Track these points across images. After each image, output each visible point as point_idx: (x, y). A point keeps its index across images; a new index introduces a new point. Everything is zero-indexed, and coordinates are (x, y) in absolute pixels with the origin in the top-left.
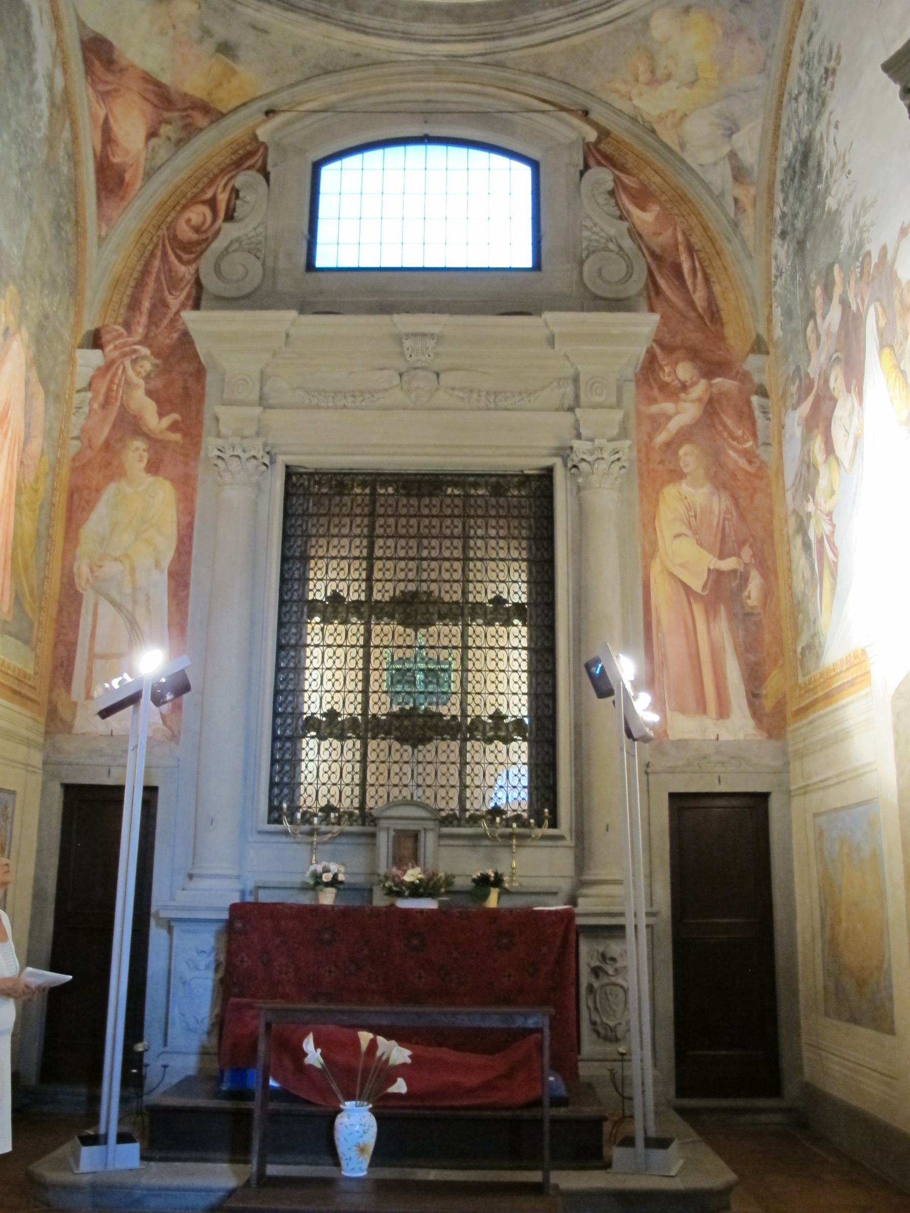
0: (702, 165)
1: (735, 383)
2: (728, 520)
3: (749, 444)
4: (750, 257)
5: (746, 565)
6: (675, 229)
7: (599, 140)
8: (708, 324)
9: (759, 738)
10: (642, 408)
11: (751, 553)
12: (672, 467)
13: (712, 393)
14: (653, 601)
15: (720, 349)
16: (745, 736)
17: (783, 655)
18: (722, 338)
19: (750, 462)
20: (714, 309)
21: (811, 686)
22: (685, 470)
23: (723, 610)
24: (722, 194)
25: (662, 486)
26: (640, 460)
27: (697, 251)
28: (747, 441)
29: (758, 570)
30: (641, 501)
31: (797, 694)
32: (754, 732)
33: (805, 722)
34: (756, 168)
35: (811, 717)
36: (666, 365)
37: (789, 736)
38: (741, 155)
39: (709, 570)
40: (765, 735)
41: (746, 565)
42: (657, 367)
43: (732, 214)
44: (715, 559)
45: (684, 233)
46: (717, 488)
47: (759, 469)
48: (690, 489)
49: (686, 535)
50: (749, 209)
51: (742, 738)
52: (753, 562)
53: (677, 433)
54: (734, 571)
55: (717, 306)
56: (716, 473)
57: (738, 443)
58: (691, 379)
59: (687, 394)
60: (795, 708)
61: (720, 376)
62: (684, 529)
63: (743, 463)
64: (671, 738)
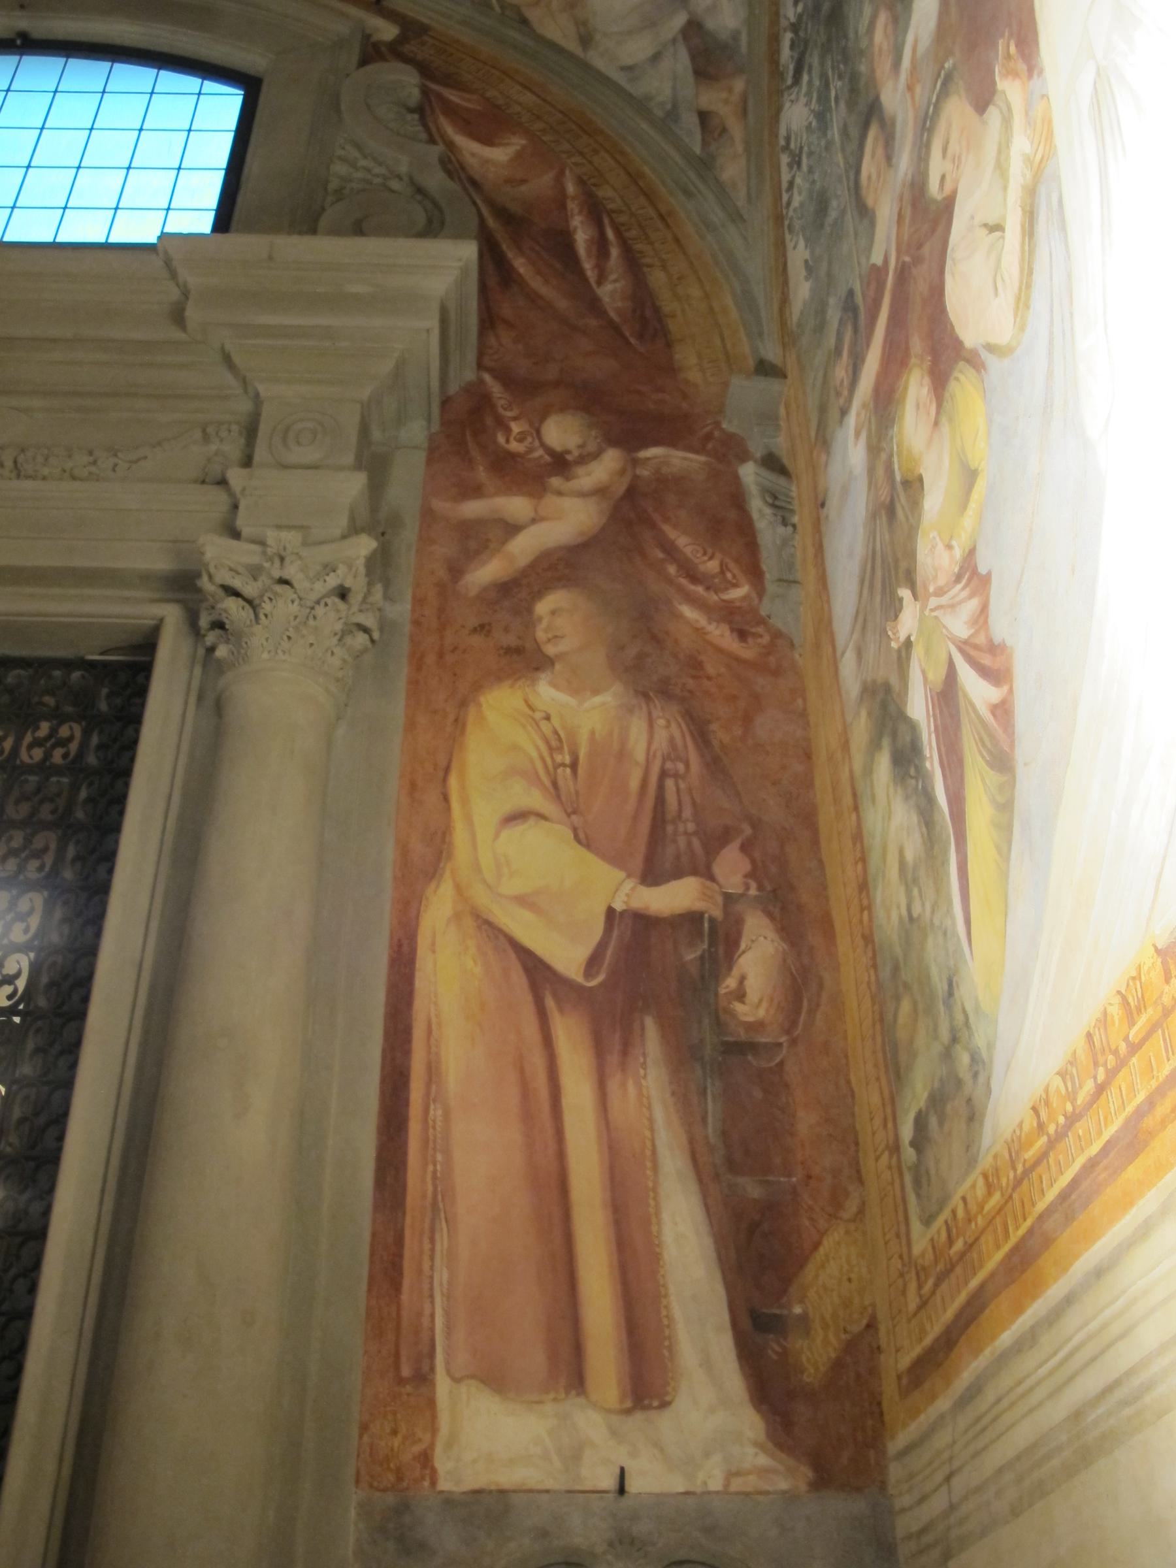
0: (624, 69)
1: (703, 458)
2: (676, 776)
4: (736, 217)
5: (728, 898)
6: (562, 173)
7: (402, 39)
8: (632, 340)
9: (783, 1485)
10: (440, 505)
11: (746, 866)
12: (510, 640)
13: (636, 477)
16: (730, 1475)
17: (861, 1181)
18: (671, 370)
19: (742, 635)
20: (648, 313)
21: (959, 1245)
22: (551, 650)
23: (651, 1029)
24: (673, 114)
25: (477, 687)
26: (416, 623)
27: (609, 213)
28: (736, 586)
29: (770, 916)
30: (411, 725)
31: (913, 1303)
32: (763, 1460)
33: (943, 1404)
34: (744, 38)
35: (969, 1371)
36: (515, 419)
38: (710, 24)
39: (610, 912)
40: (806, 1472)
41: (729, 899)
42: (489, 421)
43: (697, 149)
44: (629, 884)
45: (581, 181)
47: (770, 649)
48: (563, 697)
50: (736, 130)
51: (716, 1485)
52: (753, 892)
53: (533, 566)
54: (693, 919)
55: (657, 310)
56: (641, 656)
57: (708, 588)
58: (581, 446)
60: (905, 1361)
62: (536, 799)
63: (721, 635)
64: (444, 1485)
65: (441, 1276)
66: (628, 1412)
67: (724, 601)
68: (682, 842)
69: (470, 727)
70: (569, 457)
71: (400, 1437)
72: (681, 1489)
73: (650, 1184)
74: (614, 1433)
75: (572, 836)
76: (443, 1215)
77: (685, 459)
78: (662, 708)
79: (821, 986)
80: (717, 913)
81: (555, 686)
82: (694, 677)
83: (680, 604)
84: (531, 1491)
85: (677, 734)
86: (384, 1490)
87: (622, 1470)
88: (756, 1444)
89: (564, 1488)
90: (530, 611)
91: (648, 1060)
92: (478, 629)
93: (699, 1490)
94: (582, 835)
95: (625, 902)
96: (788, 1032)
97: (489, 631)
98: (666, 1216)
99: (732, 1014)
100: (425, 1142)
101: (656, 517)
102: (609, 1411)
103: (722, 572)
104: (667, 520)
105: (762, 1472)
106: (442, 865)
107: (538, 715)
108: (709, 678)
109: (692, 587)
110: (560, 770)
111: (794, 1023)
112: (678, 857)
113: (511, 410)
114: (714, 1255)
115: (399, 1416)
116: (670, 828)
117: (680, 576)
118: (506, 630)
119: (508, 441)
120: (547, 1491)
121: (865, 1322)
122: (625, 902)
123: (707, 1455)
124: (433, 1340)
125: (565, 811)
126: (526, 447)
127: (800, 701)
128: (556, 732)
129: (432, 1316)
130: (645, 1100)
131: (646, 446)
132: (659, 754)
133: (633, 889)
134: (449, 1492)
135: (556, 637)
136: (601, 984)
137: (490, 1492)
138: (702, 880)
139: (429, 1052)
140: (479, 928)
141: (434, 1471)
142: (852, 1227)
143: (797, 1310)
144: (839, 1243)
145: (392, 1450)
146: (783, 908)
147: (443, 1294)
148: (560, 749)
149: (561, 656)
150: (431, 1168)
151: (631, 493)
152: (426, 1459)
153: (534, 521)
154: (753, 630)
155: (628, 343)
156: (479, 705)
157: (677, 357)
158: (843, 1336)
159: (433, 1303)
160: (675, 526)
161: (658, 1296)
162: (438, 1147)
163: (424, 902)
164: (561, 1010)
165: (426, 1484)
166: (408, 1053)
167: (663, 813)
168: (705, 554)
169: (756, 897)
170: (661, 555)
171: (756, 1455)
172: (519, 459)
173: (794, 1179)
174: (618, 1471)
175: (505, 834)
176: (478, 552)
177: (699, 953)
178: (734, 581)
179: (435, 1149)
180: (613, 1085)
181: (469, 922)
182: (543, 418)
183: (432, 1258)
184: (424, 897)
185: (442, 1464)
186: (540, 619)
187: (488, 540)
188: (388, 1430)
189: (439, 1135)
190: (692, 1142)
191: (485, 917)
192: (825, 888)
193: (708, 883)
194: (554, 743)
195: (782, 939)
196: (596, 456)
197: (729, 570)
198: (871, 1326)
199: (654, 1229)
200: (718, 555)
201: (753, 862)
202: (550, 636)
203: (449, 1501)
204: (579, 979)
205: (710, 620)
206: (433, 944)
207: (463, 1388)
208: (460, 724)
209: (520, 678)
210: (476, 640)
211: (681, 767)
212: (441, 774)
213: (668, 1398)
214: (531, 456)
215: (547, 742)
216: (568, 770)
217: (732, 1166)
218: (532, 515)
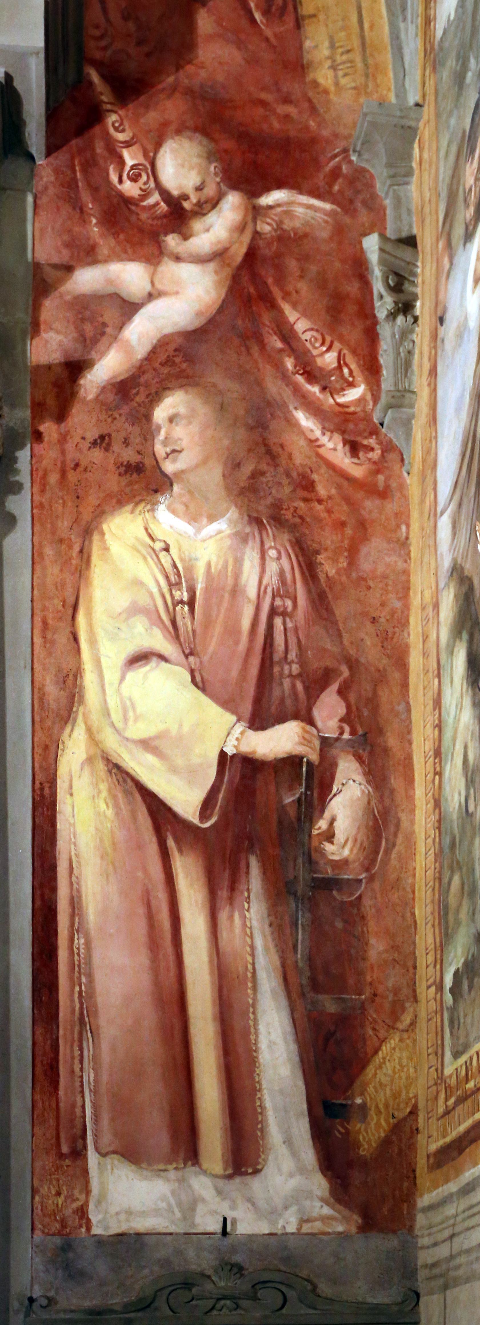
1: (327, 206)
2: (284, 614)
3: (353, 395)
5: (325, 741)
8: (258, 16)
11: (341, 710)
12: (129, 455)
13: (256, 233)
14: (62, 844)
15: (287, 100)
16: (303, 1221)
17: (416, 1000)
19: (354, 448)
22: (169, 467)
25: (100, 513)
28: (352, 385)
29: (359, 759)
32: (327, 1211)
36: (128, 144)
37: (421, 1220)
39: (223, 754)
41: (325, 741)
42: (99, 148)
44: (239, 728)
46: (256, 521)
47: (378, 468)
49: (162, 658)
51: (291, 1229)
52: (346, 736)
56: (256, 475)
57: (324, 389)
58: (199, 189)
59: (186, 237)
61: (280, 185)
64: (96, 1231)
65: (89, 1076)
66: (230, 1177)
67: (338, 404)
68: (287, 683)
69: (95, 559)
70: (186, 205)
71: (62, 1197)
72: (267, 1232)
73: (251, 1001)
74: (219, 1192)
75: (189, 678)
76: (88, 1028)
77: (309, 207)
78: (274, 535)
79: (398, 826)
80: (314, 757)
81: (174, 512)
82: (306, 500)
83: (296, 408)
84: (159, 1234)
85: (287, 567)
86: (54, 1235)
87: (225, 1219)
88: (322, 1200)
89: (182, 1231)
90: (148, 417)
91: (252, 895)
92: (99, 441)
93: (280, 1232)
94: (198, 679)
95: (235, 747)
96: (367, 870)
97: (109, 445)
98: (262, 1028)
99: (322, 853)
100: (72, 966)
101: (277, 293)
102: (216, 1176)
103: (340, 367)
104: (286, 295)
105: (324, 1219)
106: (74, 709)
107: (158, 546)
108: (320, 501)
109: (309, 387)
110: (178, 608)
111: (373, 861)
112: (282, 700)
113: (123, 131)
114: (297, 1059)
115: (61, 1182)
116: (276, 669)
117: (297, 373)
118: (126, 442)
119: (121, 181)
120: (171, 1234)
121: (408, 1110)
122: (235, 747)
123: (286, 1208)
124: (85, 1126)
125: (184, 652)
126: (141, 189)
127: (404, 528)
128: (175, 566)
129: (83, 1107)
130: (248, 931)
131: (268, 189)
132: (269, 590)
133: (242, 733)
134: (100, 1235)
135: (174, 451)
136: (213, 826)
137: (130, 1234)
138: (303, 724)
139: (72, 889)
140: (110, 772)
141: (89, 1221)
142: (405, 1035)
143: (359, 1101)
144: (394, 1049)
145: (57, 1205)
146: (371, 753)
147: (90, 1090)
148: (179, 584)
149: (179, 474)
150: (77, 988)
151: (251, 255)
152: (82, 1212)
153: (151, 297)
154: (365, 442)
155: (253, 21)
156: (103, 534)
157: (308, 44)
158: (391, 1121)
159: (83, 1097)
160: (294, 306)
161: (255, 1090)
162: (82, 971)
163: (61, 746)
164: (180, 851)
165: (83, 1230)
166: (54, 889)
167: (271, 654)
168: (323, 344)
169: (349, 740)
170: (279, 345)
171: (322, 1206)
172: (133, 208)
173: (363, 997)
174: (222, 1219)
175: (130, 675)
176: (95, 341)
177: (297, 796)
178: (351, 379)
179: (79, 973)
180: (223, 916)
181: (101, 766)
182: (158, 145)
183: (81, 1061)
184: (60, 742)
185: (94, 1216)
186: (159, 428)
187: (104, 325)
188: (54, 1193)
189: (82, 961)
190: (283, 965)
191: (114, 761)
192: (409, 732)
193: (308, 727)
194: (173, 578)
195: (369, 782)
196: (215, 203)
197: (347, 365)
198: (414, 1112)
199: (252, 1037)
200: (337, 345)
201: (348, 707)
202: (168, 450)
203: (100, 1241)
204: (196, 821)
205: (324, 430)
206: (71, 787)
207: (108, 1160)
208: (85, 556)
209: (141, 501)
210: (97, 455)
211: (289, 603)
212: (70, 612)
213: (259, 1167)
214: (145, 203)
215: (167, 577)
216: (186, 608)
217: (315, 986)
218: (148, 287)
